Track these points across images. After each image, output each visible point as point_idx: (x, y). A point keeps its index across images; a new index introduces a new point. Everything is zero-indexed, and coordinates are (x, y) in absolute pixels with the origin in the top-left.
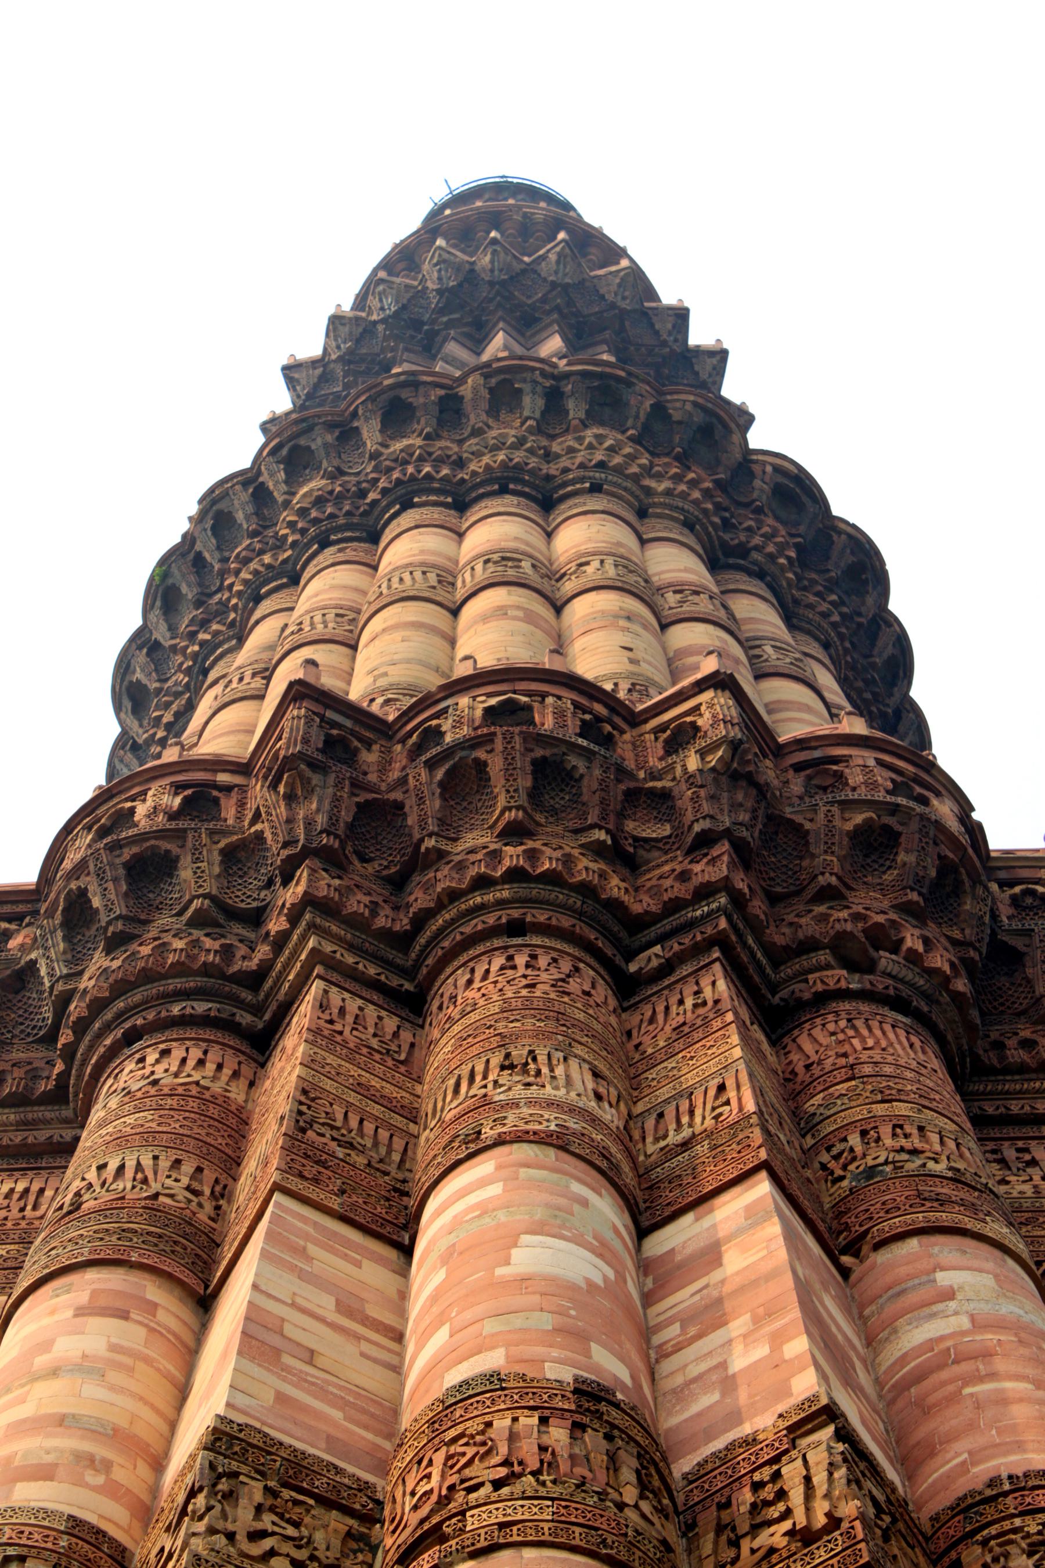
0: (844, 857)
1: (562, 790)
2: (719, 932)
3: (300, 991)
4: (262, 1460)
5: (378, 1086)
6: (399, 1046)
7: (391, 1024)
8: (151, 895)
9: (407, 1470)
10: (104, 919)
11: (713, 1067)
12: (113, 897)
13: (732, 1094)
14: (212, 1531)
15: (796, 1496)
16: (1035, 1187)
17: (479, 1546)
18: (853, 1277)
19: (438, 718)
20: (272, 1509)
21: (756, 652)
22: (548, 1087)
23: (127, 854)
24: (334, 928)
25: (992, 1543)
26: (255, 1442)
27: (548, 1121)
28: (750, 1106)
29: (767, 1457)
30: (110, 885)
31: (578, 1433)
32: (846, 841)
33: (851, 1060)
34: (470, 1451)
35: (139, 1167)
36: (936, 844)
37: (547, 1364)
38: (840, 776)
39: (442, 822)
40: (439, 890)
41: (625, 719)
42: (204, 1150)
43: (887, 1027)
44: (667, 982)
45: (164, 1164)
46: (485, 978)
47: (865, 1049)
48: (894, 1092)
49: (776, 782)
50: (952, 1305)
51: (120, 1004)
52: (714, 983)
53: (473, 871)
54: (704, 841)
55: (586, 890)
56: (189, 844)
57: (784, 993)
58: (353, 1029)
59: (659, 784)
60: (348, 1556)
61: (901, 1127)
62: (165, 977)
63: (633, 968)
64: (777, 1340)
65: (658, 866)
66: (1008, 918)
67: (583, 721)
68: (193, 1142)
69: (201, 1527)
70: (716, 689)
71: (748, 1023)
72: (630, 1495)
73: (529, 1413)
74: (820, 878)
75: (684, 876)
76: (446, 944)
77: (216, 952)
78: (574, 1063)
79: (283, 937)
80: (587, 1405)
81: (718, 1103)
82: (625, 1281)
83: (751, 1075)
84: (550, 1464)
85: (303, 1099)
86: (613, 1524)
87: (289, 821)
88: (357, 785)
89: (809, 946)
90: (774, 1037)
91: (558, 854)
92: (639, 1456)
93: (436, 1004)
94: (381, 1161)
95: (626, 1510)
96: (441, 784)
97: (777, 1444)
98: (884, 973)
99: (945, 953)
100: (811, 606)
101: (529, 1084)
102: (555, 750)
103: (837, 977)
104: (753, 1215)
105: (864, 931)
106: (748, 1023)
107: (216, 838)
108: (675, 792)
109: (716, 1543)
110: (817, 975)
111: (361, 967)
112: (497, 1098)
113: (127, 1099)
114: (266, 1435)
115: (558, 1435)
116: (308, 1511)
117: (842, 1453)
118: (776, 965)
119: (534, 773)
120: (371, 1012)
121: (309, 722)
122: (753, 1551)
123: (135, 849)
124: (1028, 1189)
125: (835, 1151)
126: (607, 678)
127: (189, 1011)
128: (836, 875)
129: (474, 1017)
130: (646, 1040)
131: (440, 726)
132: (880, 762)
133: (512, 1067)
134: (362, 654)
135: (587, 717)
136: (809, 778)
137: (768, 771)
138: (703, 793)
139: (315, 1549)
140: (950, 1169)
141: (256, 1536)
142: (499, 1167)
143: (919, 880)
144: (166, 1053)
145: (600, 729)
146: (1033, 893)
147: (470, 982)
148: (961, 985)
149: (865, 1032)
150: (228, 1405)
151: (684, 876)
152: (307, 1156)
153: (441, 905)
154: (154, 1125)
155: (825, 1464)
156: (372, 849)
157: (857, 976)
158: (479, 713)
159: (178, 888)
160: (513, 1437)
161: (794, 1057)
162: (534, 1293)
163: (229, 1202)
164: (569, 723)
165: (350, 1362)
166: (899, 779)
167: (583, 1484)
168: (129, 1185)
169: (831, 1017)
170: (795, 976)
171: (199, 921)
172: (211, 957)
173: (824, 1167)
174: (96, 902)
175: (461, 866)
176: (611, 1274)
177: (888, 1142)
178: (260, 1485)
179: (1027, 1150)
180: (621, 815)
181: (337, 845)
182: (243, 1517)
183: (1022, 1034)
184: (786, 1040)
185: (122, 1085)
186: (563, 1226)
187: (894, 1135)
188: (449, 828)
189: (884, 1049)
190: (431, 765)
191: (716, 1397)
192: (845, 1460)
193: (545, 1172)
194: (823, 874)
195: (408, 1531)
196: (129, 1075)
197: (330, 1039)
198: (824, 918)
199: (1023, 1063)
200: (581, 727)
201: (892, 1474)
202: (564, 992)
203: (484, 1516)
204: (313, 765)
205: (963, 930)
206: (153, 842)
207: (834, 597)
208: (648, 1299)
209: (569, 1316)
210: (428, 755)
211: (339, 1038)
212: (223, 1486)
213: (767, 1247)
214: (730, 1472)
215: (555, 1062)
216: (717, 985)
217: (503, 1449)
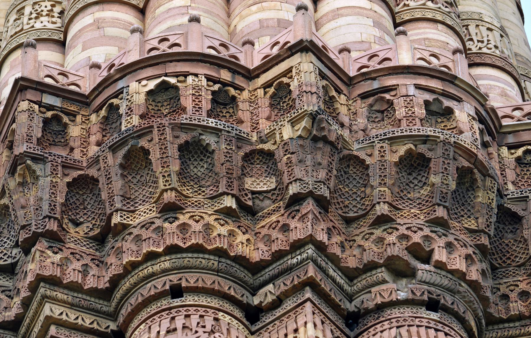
0: (393, 184)
2: (308, 278)
19: (116, 97)
38: (390, 103)
54: (297, 200)
59: (266, 147)
67: (213, 93)
75: (285, 228)
111: (80, 321)
135: (216, 87)
145: (226, 92)
157: (404, 281)
169: (386, 325)
204: (36, 159)
205: (477, 218)
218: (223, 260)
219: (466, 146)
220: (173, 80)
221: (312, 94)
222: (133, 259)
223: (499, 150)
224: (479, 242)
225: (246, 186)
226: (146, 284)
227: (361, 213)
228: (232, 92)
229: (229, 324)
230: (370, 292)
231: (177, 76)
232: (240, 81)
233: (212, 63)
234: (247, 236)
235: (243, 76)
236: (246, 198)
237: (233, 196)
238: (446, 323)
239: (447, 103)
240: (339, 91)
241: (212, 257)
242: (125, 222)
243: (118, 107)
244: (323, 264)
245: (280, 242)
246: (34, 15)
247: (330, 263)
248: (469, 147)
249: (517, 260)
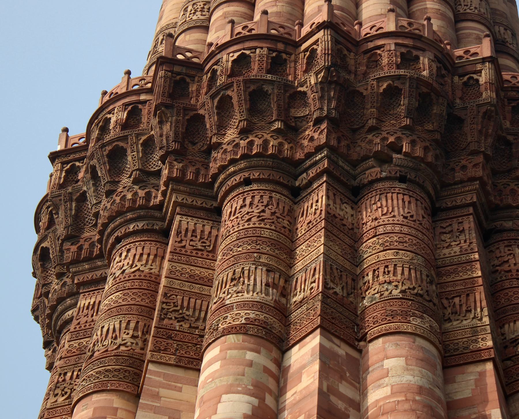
1: (264, 100)
19: (216, 64)
35: (114, 330)
42: (140, 310)
43: (395, 195)
45: (124, 325)
47: (383, 215)
50: (387, 379)
52: (322, 196)
63: (297, 184)
67: (273, 58)
68: (135, 307)
98: (395, 165)
103: (376, 171)
111: (194, 203)
112: (228, 302)
145: (281, 57)
146: (472, 78)
158: (230, 64)
180: (287, 110)
184: (359, 203)
204: (167, 106)
205: (433, 123)
206: (116, 143)
213: (314, 377)
215: (251, 274)
218: (275, 161)
219: (425, 79)
220: (247, 52)
222: (223, 164)
223: (452, 78)
224: (434, 138)
225: (291, 114)
226: (231, 178)
227: (361, 125)
228: (284, 56)
229: (279, 199)
230: (365, 174)
231: (250, 49)
232: (290, 49)
233: (272, 40)
234: (291, 145)
235: (292, 45)
236: (291, 121)
237: (282, 121)
238: (411, 189)
239: (415, 53)
240: (349, 51)
241: (268, 160)
242: (219, 141)
243: (217, 70)
244: (335, 159)
245: (309, 147)
246: (193, 11)
247: (340, 158)
248: (427, 80)
249: (461, 146)
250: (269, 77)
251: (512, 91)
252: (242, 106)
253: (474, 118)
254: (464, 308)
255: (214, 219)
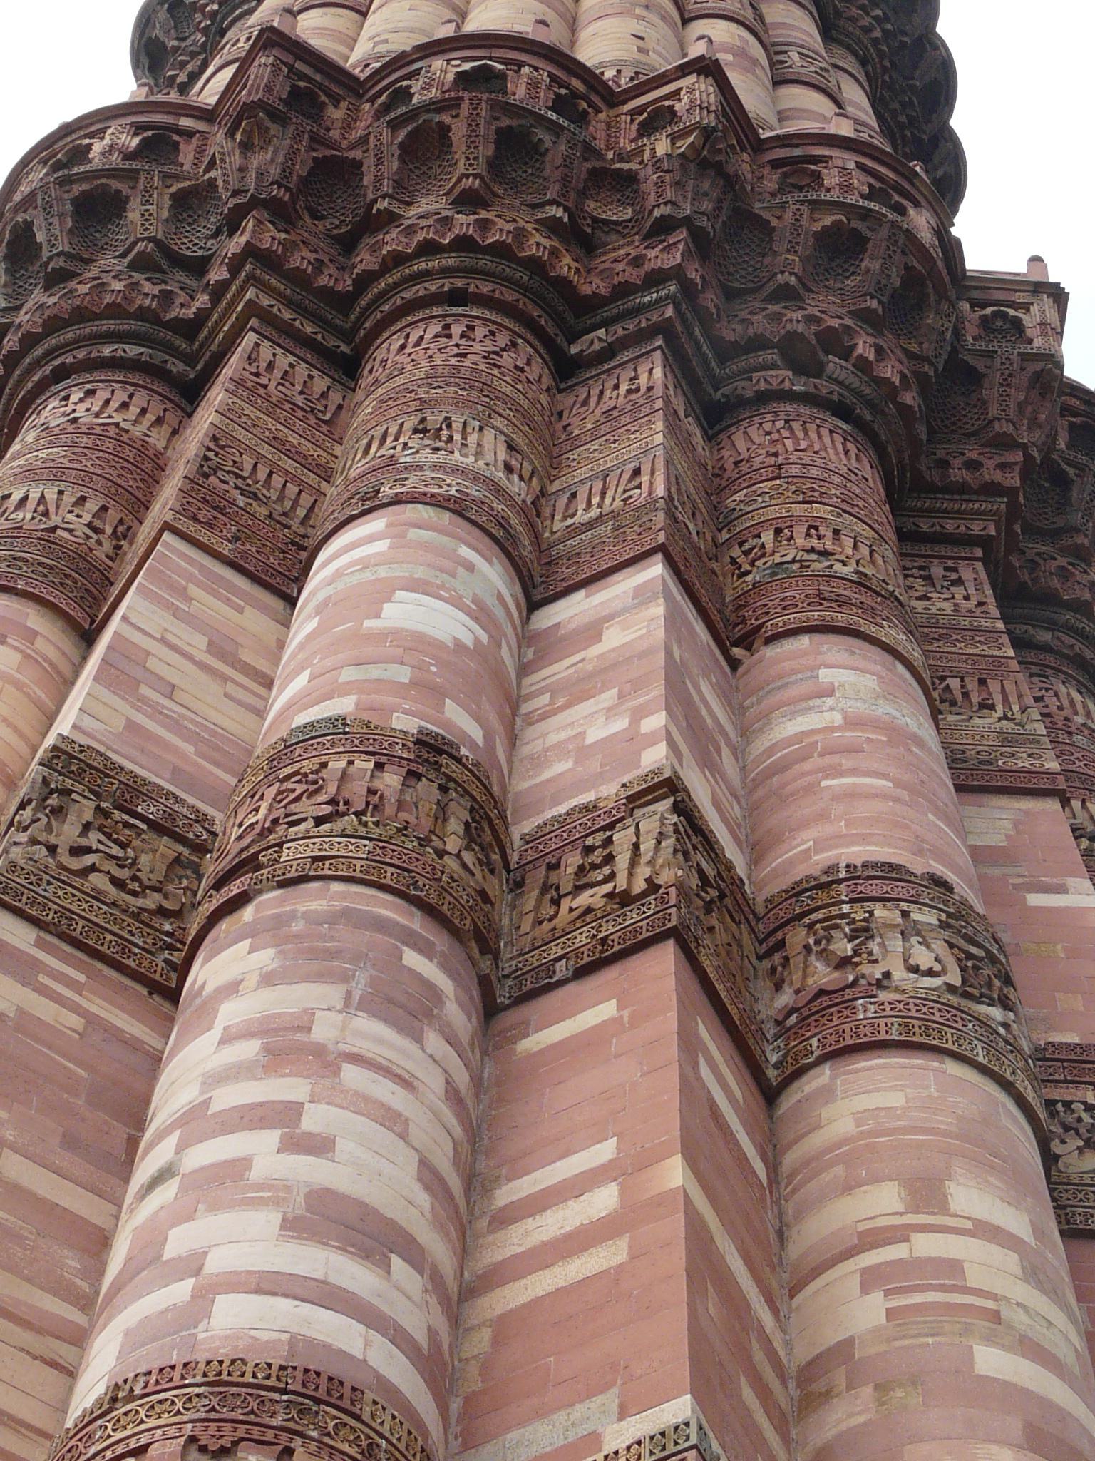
0: (808, 258)
1: (526, 163)
3: (234, 343)
4: (99, 781)
5: (295, 442)
6: (326, 407)
7: (320, 384)
8: (97, 235)
9: (241, 803)
10: (45, 254)
11: (632, 451)
12: (57, 232)
13: (645, 478)
14: (34, 842)
15: (622, 861)
16: (956, 605)
17: (288, 876)
18: (741, 670)
20: (100, 829)
21: (781, 57)
22: (457, 453)
23: (77, 189)
24: (273, 280)
25: (818, 925)
26: (95, 764)
27: (449, 485)
28: (660, 491)
29: (603, 823)
30: (56, 220)
31: (412, 782)
32: (811, 241)
33: (780, 460)
34: (300, 789)
35: (42, 499)
36: (903, 253)
37: (395, 715)
38: (817, 177)
39: (398, 184)
40: (384, 252)
41: (604, 99)
42: (113, 490)
43: (825, 432)
44: (606, 367)
45: (69, 499)
46: (418, 344)
48: (816, 494)
49: (749, 176)
50: (829, 701)
51: (53, 341)
53: (420, 236)
54: (663, 227)
55: (534, 265)
56: (141, 186)
57: (726, 390)
58: (279, 384)
59: (626, 166)
60: (172, 882)
61: (816, 528)
62: (98, 317)
63: (574, 350)
64: (639, 714)
65: (615, 249)
66: (974, 338)
68: (101, 481)
69: (23, 837)
70: (699, 75)
71: (681, 413)
72: (453, 844)
73: (366, 757)
74: (779, 276)
75: (637, 261)
76: (386, 308)
77: (154, 296)
78: (489, 434)
79: (223, 286)
80: (426, 756)
81: (631, 485)
82: (499, 646)
83: (668, 462)
84: (375, 807)
85: (212, 445)
86: (429, 869)
87: (241, 170)
88: (317, 140)
89: (758, 344)
90: (710, 432)
91: (511, 227)
92: (472, 809)
93: (368, 367)
94: (284, 514)
95: (446, 857)
96: (401, 145)
97: (614, 812)
99: (897, 364)
100: (853, 20)
101: (438, 449)
102: (523, 122)
103: (782, 377)
104: (642, 596)
105: (815, 334)
106: (681, 413)
107: (169, 182)
108: (642, 175)
109: (539, 901)
110: (763, 373)
111: (297, 323)
113: (44, 434)
114: (107, 758)
115: (391, 780)
116: (139, 835)
117: (675, 824)
118: (722, 361)
119: (497, 142)
120: (302, 370)
121: (276, 69)
122: (571, 910)
123: (85, 187)
124: (948, 607)
125: (746, 547)
126: (611, 64)
127: (120, 353)
128: (796, 275)
129: (399, 380)
130: (575, 421)
131: (410, 87)
132: (860, 166)
133: (425, 431)
134: (371, 19)
135: (563, 91)
136: (785, 175)
137: (743, 164)
138: (668, 178)
139: (139, 870)
140: (857, 572)
141: (77, 851)
142: (389, 525)
143: (880, 289)
144: (90, 393)
145: (576, 105)
146: (1005, 315)
147: (403, 347)
148: (909, 398)
149: (800, 434)
150: (75, 726)
151: (637, 261)
152: (204, 501)
153: (385, 268)
154: (65, 461)
155: (655, 834)
156: (325, 206)
157: (803, 379)
158: (450, 77)
159: (125, 229)
160: (344, 777)
161: (726, 453)
162: (398, 646)
163: (131, 543)
164: (542, 94)
165: (212, 703)
166: (878, 185)
167: (406, 828)
168: (29, 516)
169: (769, 417)
170: (741, 373)
171: (142, 264)
172: (147, 302)
173: (733, 561)
174: (40, 237)
175: (410, 231)
176: (484, 637)
177: (800, 541)
178: (93, 805)
179: (955, 570)
180: (583, 194)
181: (287, 198)
182: (68, 832)
183: (969, 454)
184: (721, 436)
185: (42, 420)
186: (442, 587)
187: (808, 535)
188: (404, 191)
189: (816, 453)
190: (394, 125)
191: (569, 764)
192: (676, 831)
193: (435, 534)
194: (782, 272)
195: (229, 858)
196: (51, 412)
197: (253, 391)
198: (776, 318)
199: (964, 483)
200: (554, 101)
201: (731, 852)
202: (495, 365)
203: (301, 849)
204: (274, 115)
205: (921, 343)
206: (104, 181)
207: (879, 12)
208: (524, 670)
209: (429, 671)
210: (393, 115)
211: (262, 391)
212: (53, 801)
213: (648, 626)
214: (565, 835)
215: (469, 430)
216: (654, 372)
217: (332, 789)
221: (709, 112)
237: (566, 209)
250: (553, 116)
251: (1071, 395)
252: (476, 147)
253: (1010, 375)
254: (975, 699)
255: (336, 376)
